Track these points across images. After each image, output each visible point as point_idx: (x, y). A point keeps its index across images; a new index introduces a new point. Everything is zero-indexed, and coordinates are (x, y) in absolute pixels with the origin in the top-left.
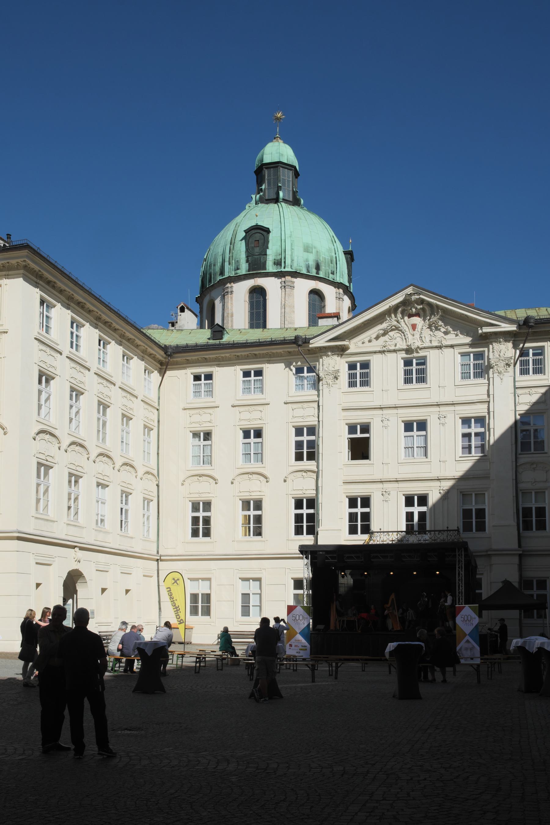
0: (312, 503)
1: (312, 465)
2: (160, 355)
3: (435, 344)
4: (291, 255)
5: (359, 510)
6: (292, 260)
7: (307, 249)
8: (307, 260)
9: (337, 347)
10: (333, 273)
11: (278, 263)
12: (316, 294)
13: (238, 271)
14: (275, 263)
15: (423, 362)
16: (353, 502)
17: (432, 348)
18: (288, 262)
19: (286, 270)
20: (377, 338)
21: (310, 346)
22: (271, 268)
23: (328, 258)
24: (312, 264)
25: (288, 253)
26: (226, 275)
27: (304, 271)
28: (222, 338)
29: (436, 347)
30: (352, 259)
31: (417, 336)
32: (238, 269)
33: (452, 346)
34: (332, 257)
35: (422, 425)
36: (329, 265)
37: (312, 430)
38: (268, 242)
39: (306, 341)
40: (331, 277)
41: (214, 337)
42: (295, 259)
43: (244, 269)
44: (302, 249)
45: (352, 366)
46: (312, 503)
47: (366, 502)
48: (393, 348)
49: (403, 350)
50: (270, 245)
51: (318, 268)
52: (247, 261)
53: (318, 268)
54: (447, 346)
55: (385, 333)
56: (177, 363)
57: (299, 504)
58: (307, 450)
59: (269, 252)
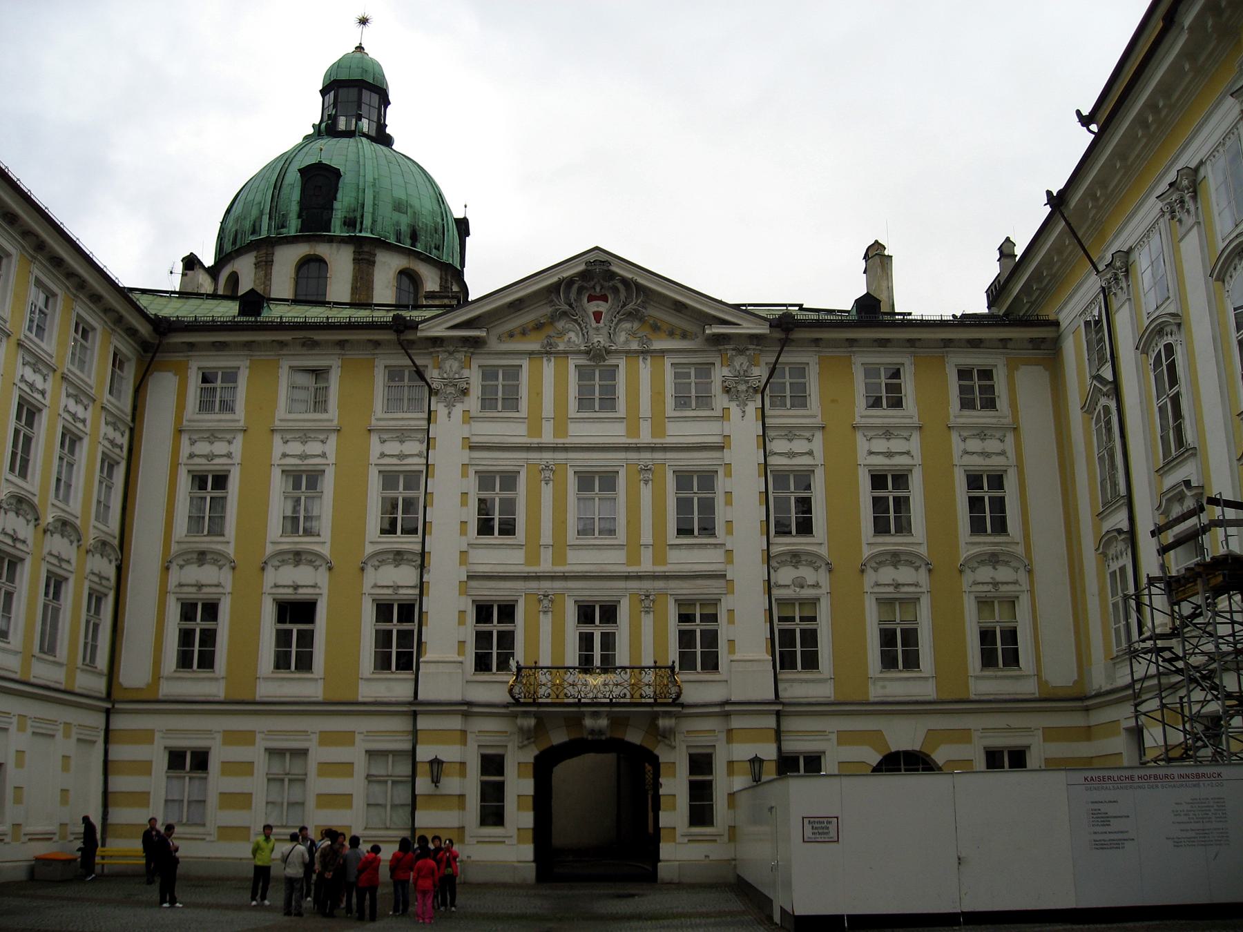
0: (408, 611)
1: (411, 543)
2: (144, 329)
3: (634, 346)
4: (373, 213)
5: (495, 627)
6: (374, 222)
7: (399, 207)
8: (398, 224)
9: (465, 340)
10: (437, 248)
11: (350, 223)
12: (409, 277)
13: (284, 230)
14: (345, 223)
15: (612, 372)
16: (483, 612)
17: (628, 352)
18: (367, 222)
19: (363, 234)
20: (539, 327)
21: (419, 334)
22: (337, 230)
23: (431, 224)
24: (404, 228)
25: (368, 208)
26: (264, 234)
27: (392, 240)
28: (259, 315)
29: (636, 352)
30: (468, 234)
31: (605, 331)
32: (283, 227)
33: (663, 352)
34: (436, 223)
35: (608, 480)
36: (432, 235)
37: (412, 479)
38: (336, 190)
39: (413, 326)
40: (434, 254)
41: (242, 312)
42: (379, 220)
43: (293, 227)
44: (390, 207)
45: (489, 374)
46: (408, 611)
47: (507, 612)
48: (561, 347)
49: (579, 352)
50: (339, 195)
51: (414, 237)
52: (299, 216)
53: (414, 237)
54: (655, 351)
55: (553, 319)
56: (175, 349)
57: (383, 611)
58: (404, 516)
59: (337, 205)
